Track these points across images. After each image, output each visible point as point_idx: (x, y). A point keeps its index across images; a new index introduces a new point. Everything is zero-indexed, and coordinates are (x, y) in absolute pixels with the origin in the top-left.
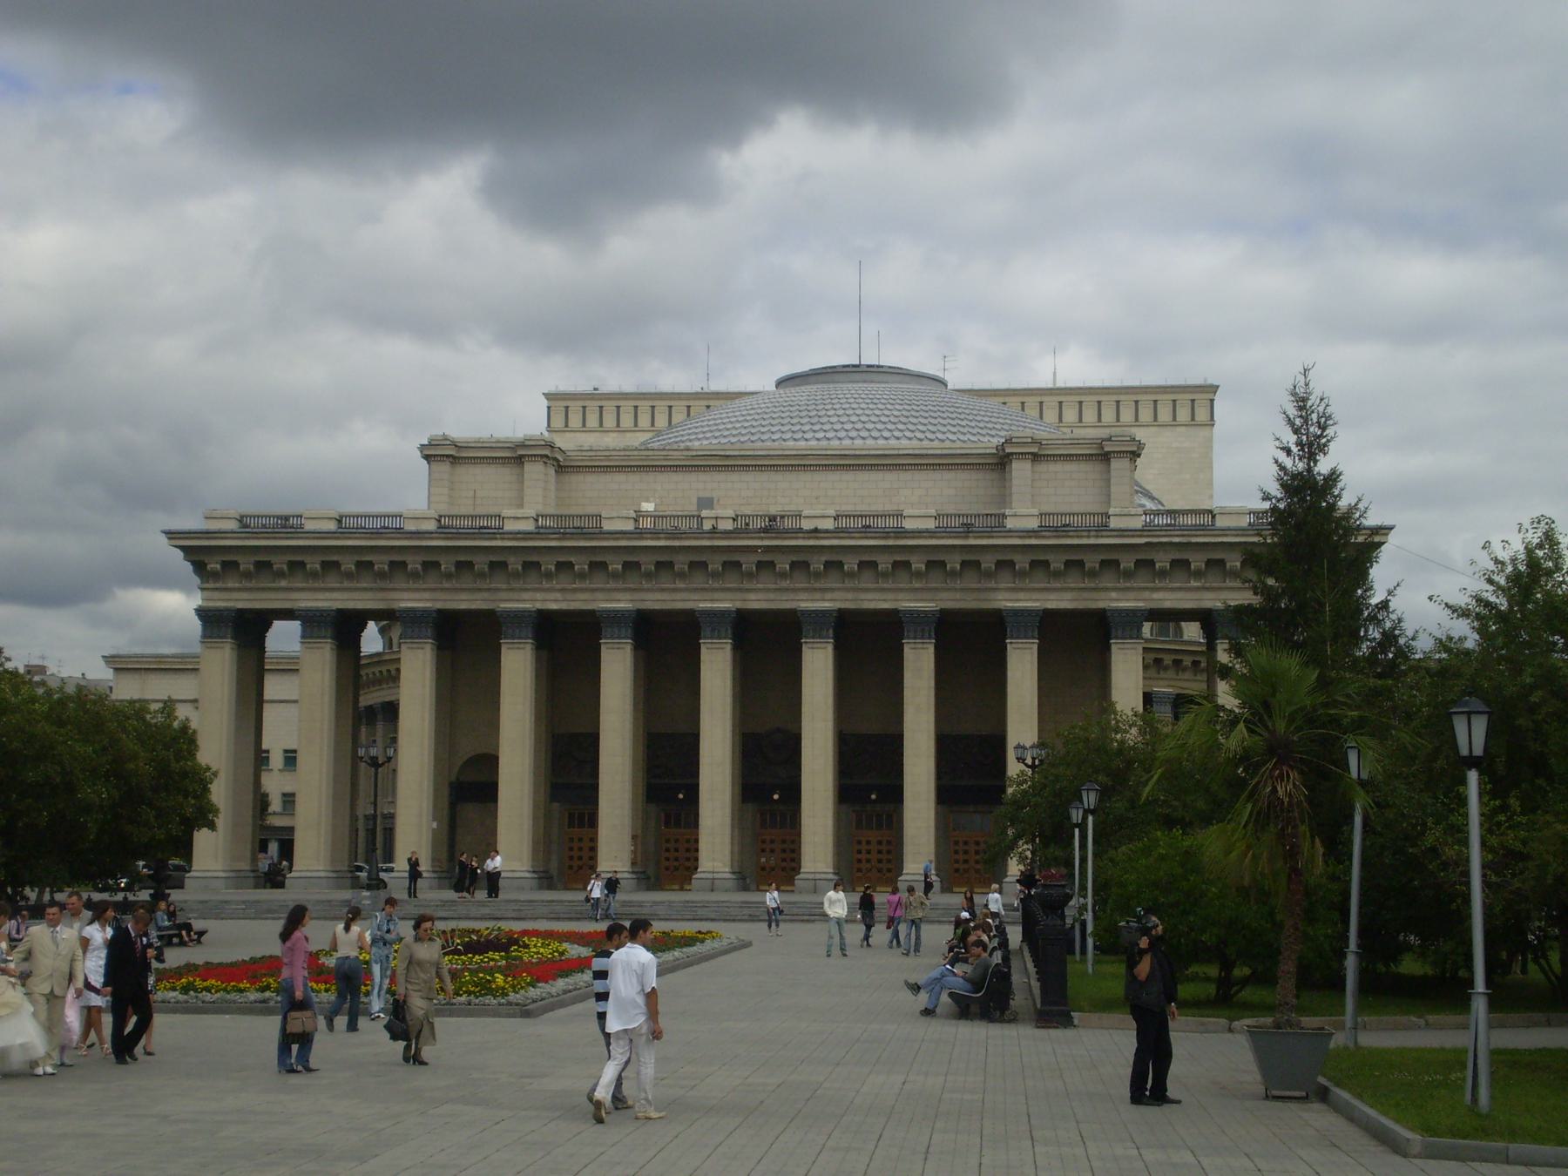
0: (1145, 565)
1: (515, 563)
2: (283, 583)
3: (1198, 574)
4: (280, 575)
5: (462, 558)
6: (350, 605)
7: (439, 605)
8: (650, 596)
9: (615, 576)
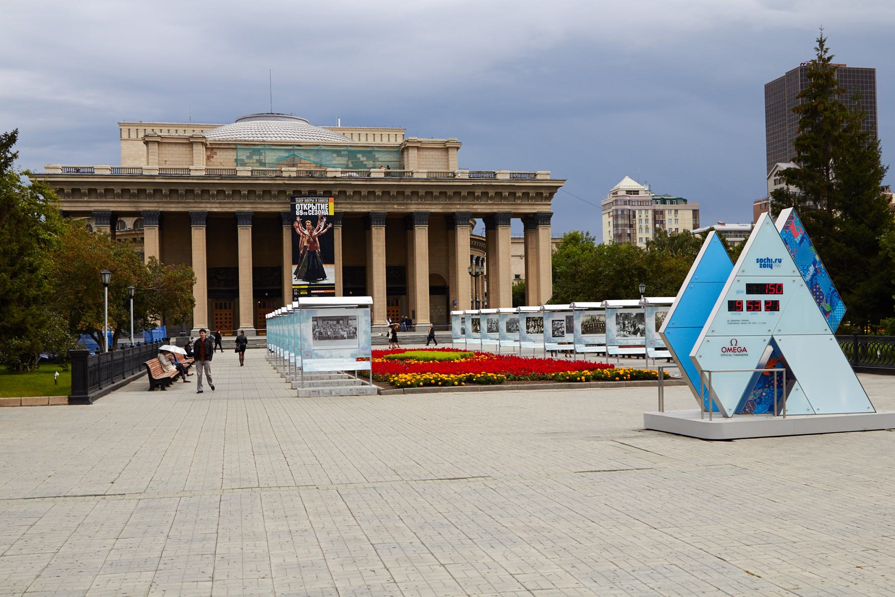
0: (471, 194)
1: (198, 191)
2: (86, 199)
3: (492, 198)
4: (84, 195)
5: (173, 188)
6: (119, 209)
7: (161, 209)
8: (259, 206)
9: (244, 196)
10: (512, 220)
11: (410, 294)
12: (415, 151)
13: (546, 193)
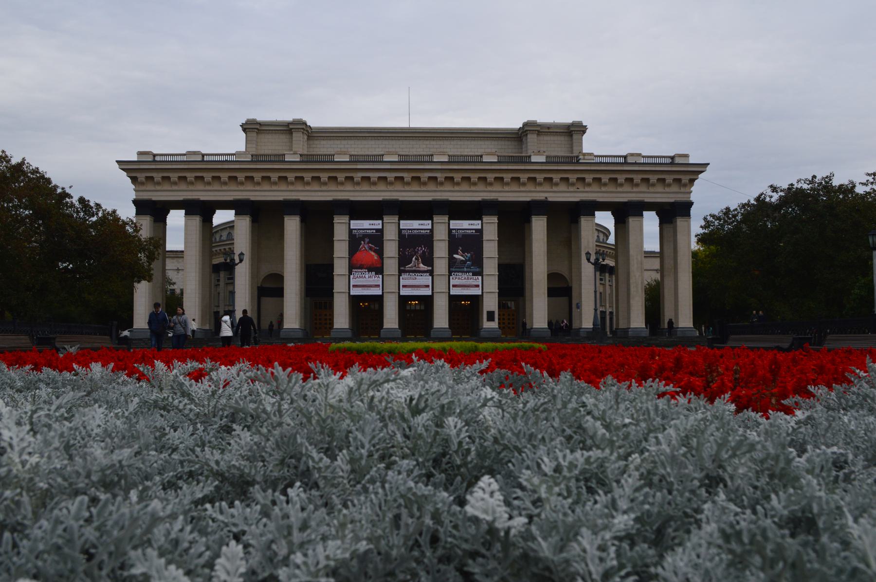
10: (645, 213)
11: (527, 294)
12: (535, 136)
13: (685, 179)
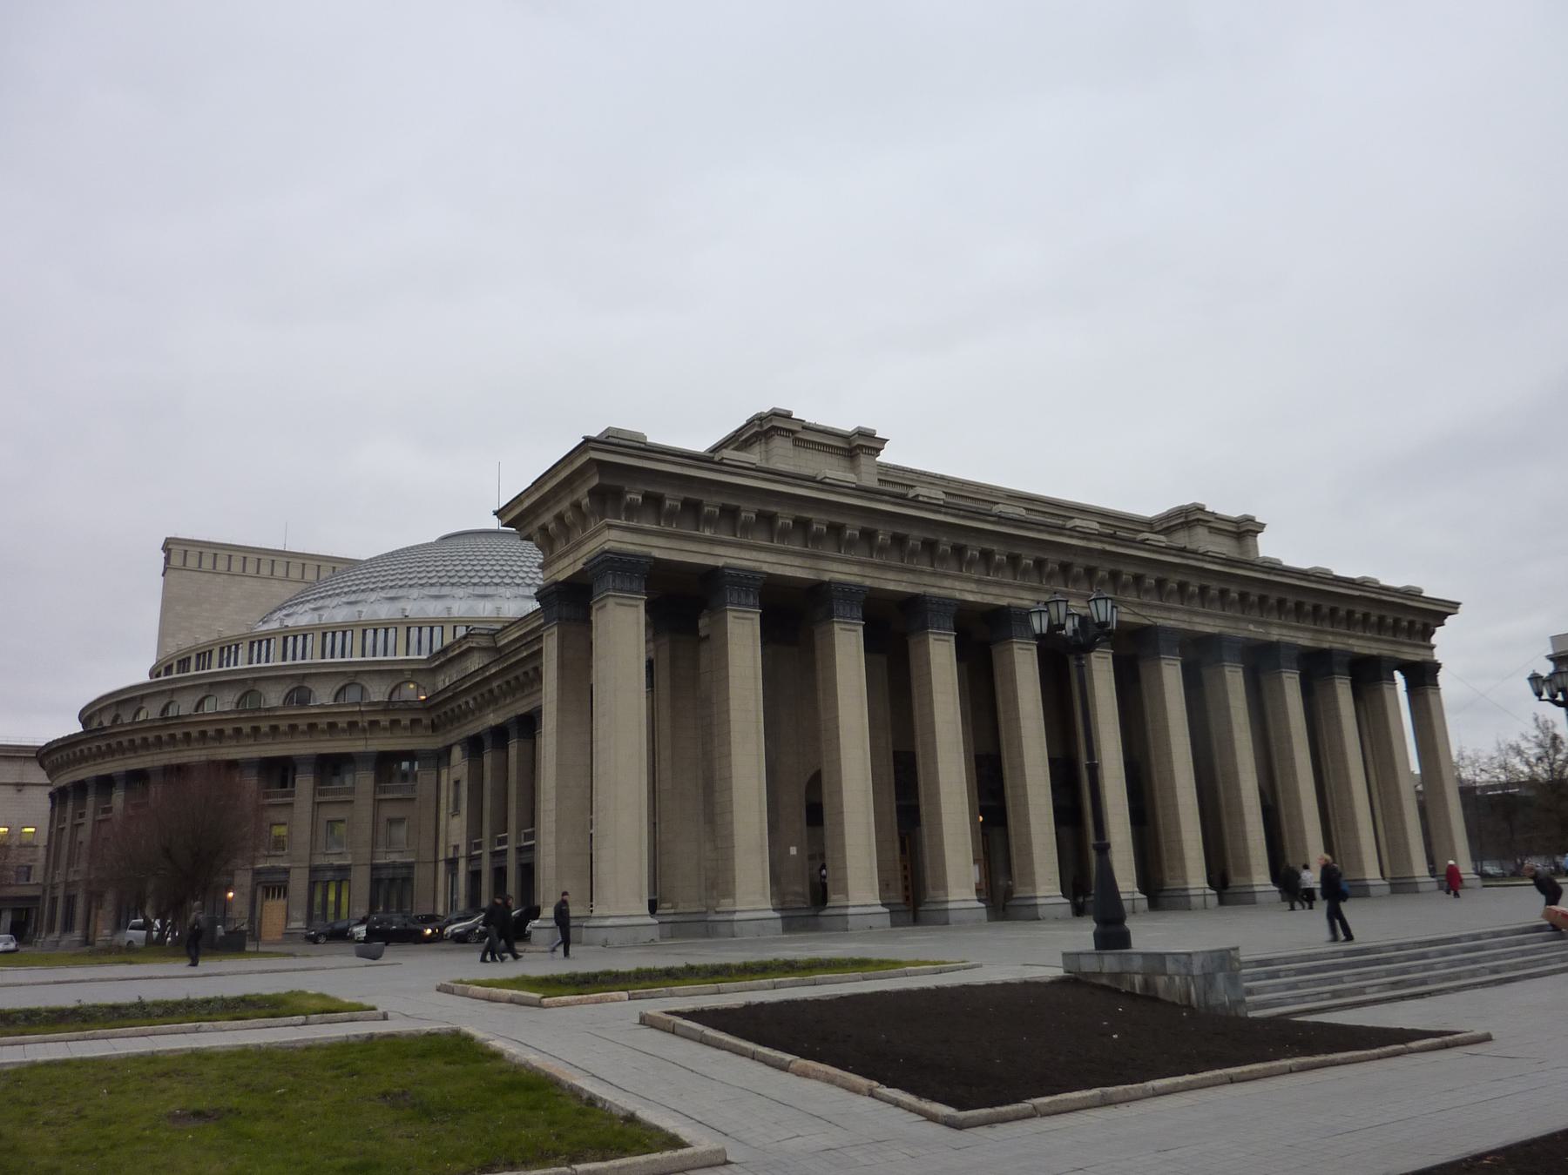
2: (707, 533)
